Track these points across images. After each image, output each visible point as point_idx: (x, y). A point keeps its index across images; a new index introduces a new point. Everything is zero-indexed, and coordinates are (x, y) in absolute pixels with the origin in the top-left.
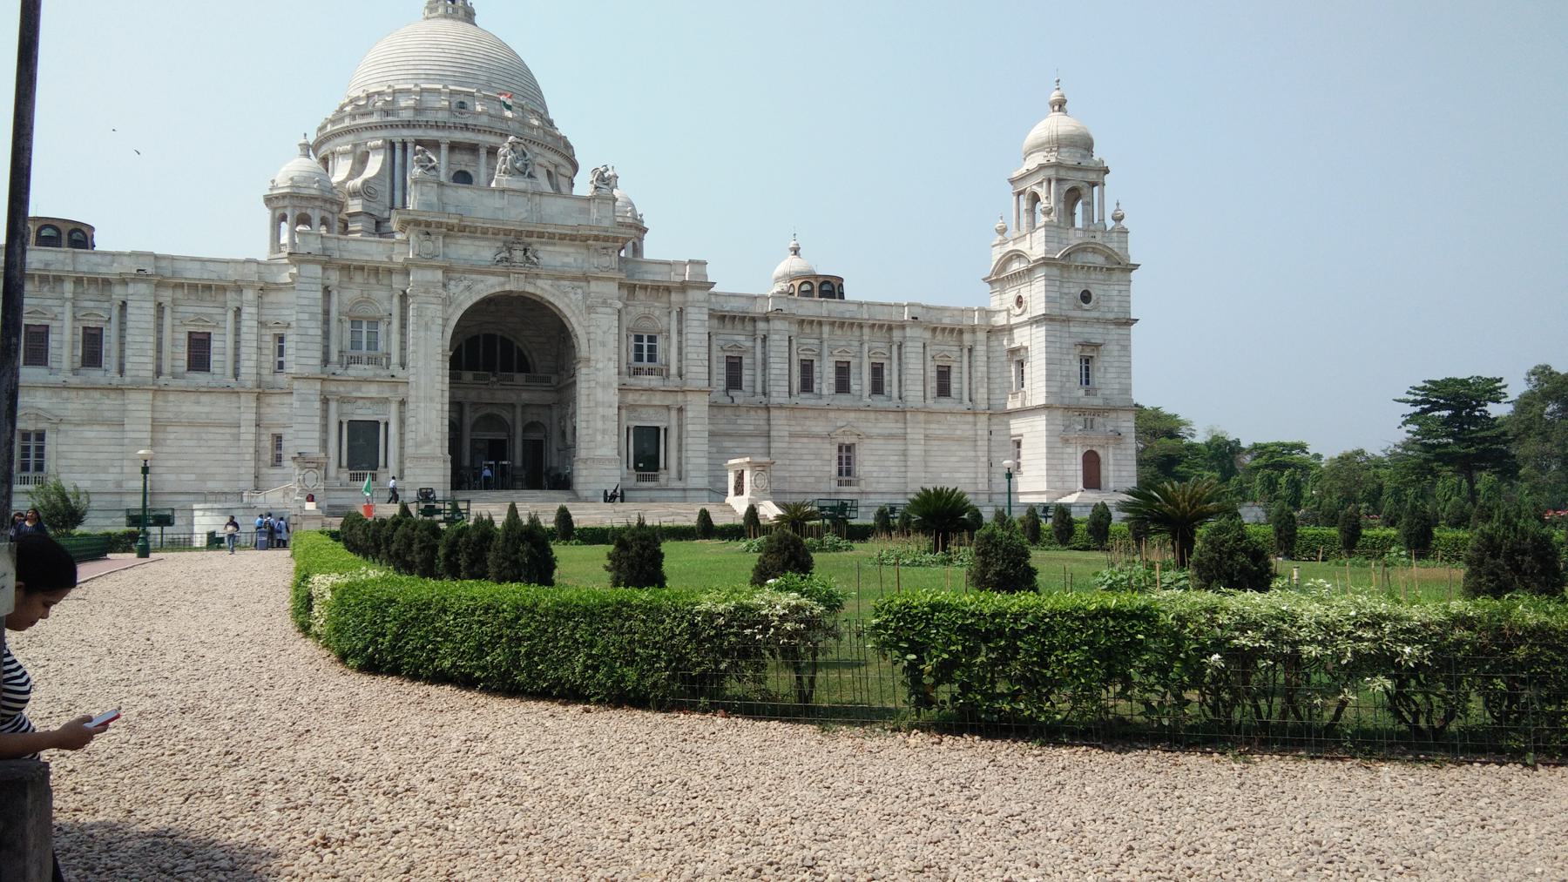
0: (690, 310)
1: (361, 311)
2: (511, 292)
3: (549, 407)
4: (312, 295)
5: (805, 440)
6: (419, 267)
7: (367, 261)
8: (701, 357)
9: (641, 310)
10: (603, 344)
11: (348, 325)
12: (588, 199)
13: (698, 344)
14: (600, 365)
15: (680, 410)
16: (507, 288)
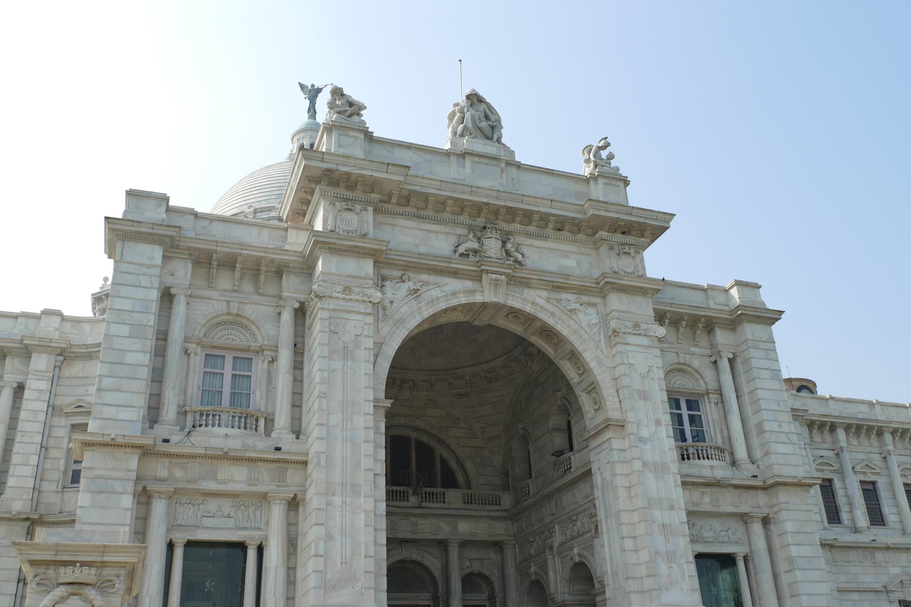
0: (753, 353)
1: (225, 337)
2: (484, 306)
3: (498, 546)
4: (140, 293)
5: (855, 596)
6: (335, 250)
7: (243, 246)
8: (785, 428)
9: (672, 358)
10: (644, 396)
11: (197, 361)
12: (586, 180)
13: (775, 407)
14: (645, 433)
15: (766, 521)
16: (478, 298)
